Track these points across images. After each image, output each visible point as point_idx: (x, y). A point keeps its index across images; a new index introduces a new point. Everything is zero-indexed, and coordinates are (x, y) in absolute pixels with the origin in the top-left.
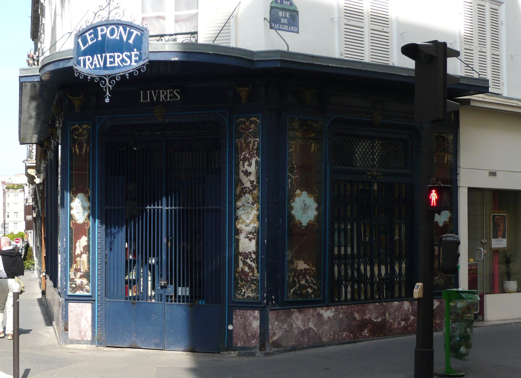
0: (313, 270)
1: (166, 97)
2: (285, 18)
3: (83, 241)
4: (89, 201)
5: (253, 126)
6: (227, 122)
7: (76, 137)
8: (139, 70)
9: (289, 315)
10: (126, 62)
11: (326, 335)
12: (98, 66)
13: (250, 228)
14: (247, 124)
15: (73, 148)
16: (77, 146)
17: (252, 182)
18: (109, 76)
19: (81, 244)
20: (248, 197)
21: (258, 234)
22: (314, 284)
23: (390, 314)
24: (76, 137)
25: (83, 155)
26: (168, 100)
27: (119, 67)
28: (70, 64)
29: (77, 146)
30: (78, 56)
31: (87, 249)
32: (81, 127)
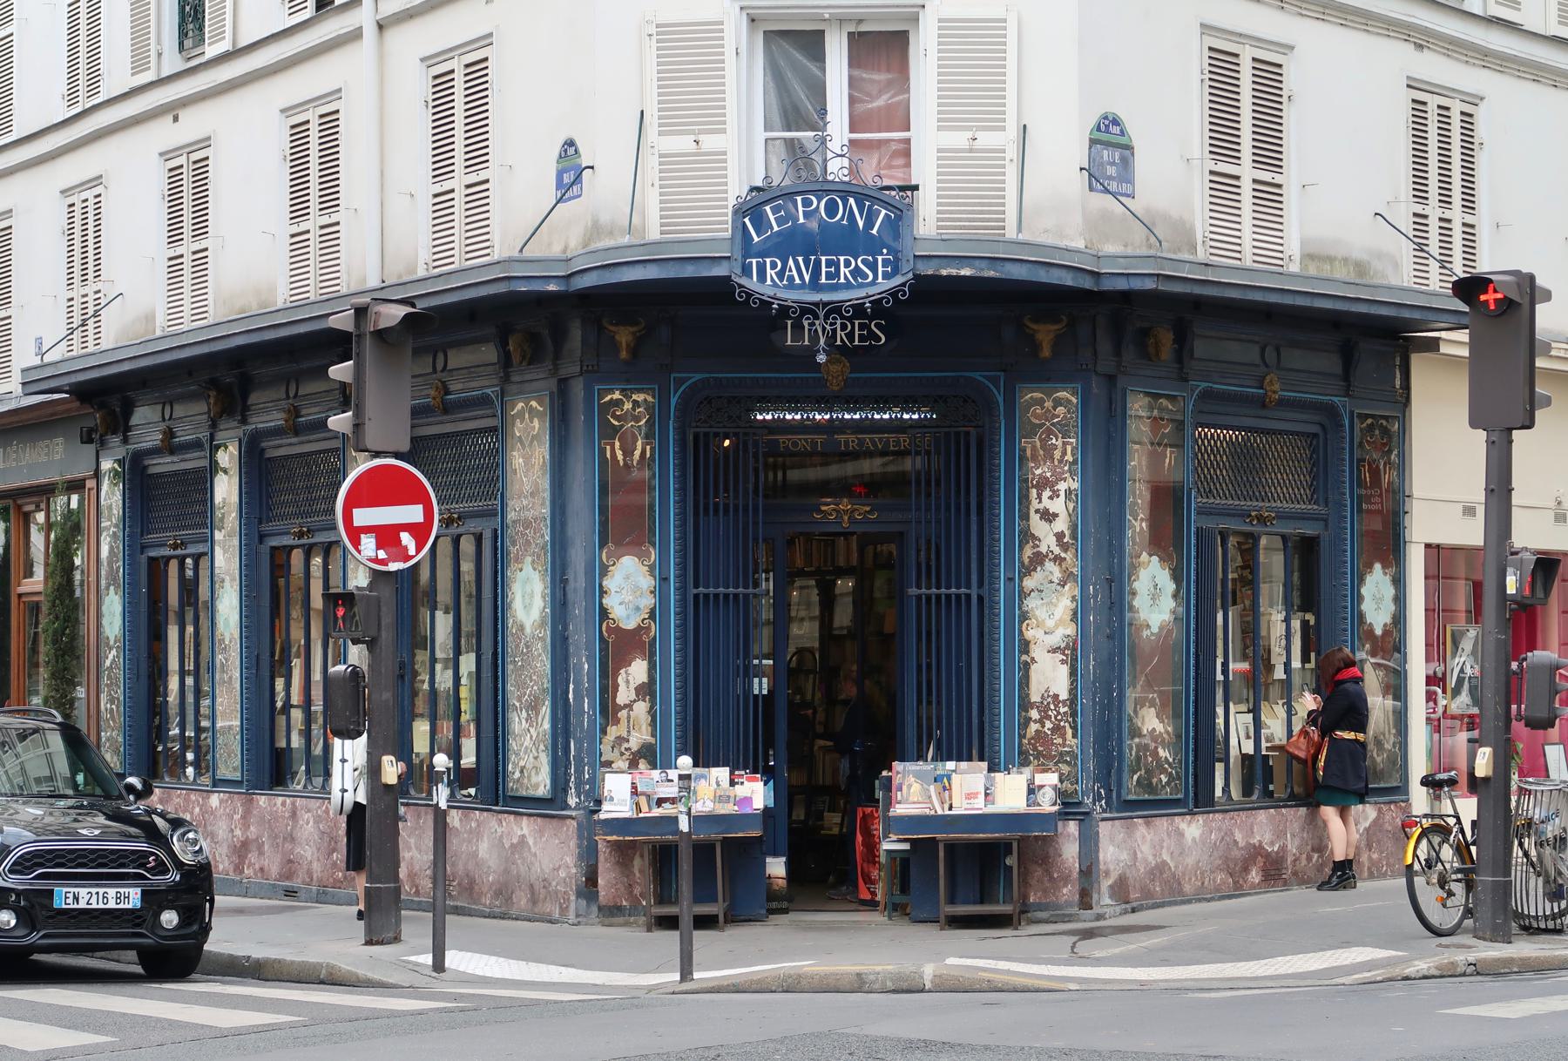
0: (1167, 732)
1: (850, 336)
2: (1113, 164)
3: (638, 671)
5: (1061, 410)
6: (1001, 400)
7: (616, 423)
8: (894, 293)
9: (1130, 831)
10: (866, 276)
11: (1190, 879)
12: (798, 281)
13: (1056, 639)
14: (1049, 404)
15: (608, 447)
16: (617, 444)
17: (1059, 536)
18: (826, 304)
19: (630, 678)
20: (1051, 569)
21: (1074, 649)
22: (1170, 764)
24: (616, 423)
25: (635, 463)
26: (856, 343)
27: (848, 286)
28: (719, 271)
29: (617, 444)
30: (745, 256)
31: (645, 691)
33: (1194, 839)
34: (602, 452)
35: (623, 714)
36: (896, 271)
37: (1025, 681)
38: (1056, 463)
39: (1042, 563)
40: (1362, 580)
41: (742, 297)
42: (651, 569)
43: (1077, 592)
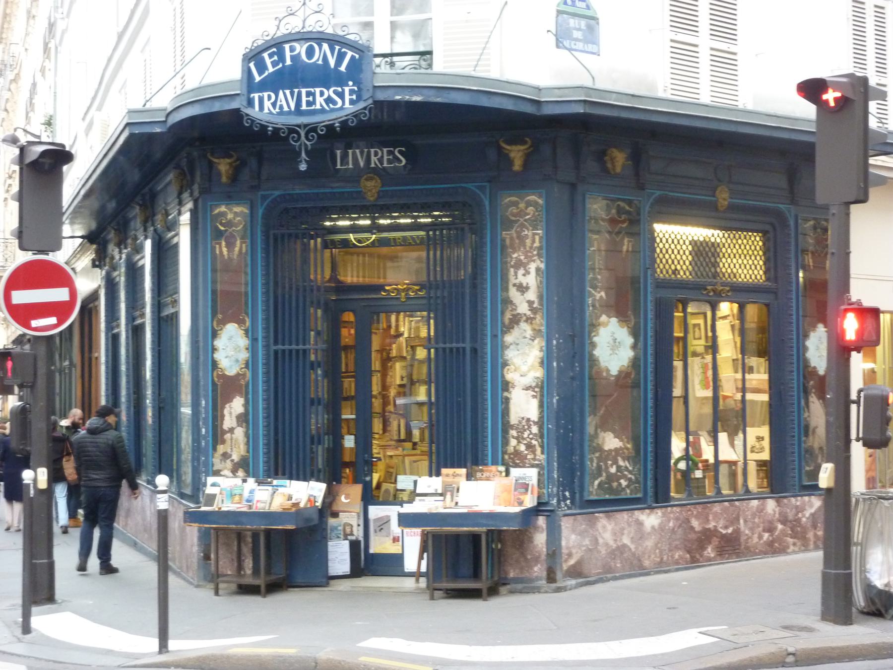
0: (627, 449)
1: (381, 160)
2: (579, 29)
3: (237, 405)
4: (247, 337)
6: (487, 203)
7: (222, 228)
8: (356, 115)
9: (592, 524)
10: (335, 103)
11: (650, 556)
12: (286, 109)
15: (217, 246)
17: (530, 303)
18: (306, 126)
20: (524, 328)
21: (542, 388)
22: (630, 472)
23: (745, 521)
24: (222, 228)
27: (323, 111)
28: (234, 105)
29: (224, 243)
30: (249, 92)
31: (243, 419)
32: (231, 210)
33: (653, 527)
34: (213, 249)
35: (228, 436)
36: (359, 98)
37: (506, 412)
38: (528, 249)
39: (517, 323)
40: (806, 336)
41: (248, 123)
42: (246, 332)
43: (544, 344)
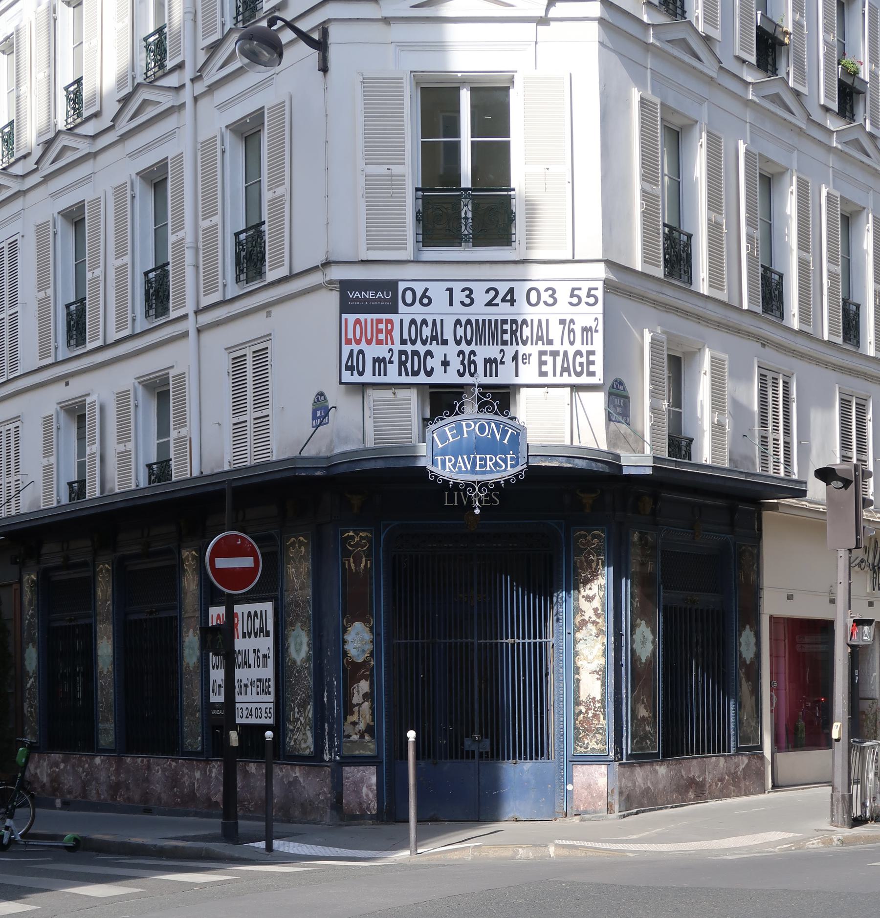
3: (364, 686)
4: (372, 633)
6: (563, 535)
7: (351, 549)
9: (632, 772)
10: (501, 467)
12: (464, 469)
14: (589, 538)
15: (347, 562)
17: (596, 610)
18: (479, 482)
19: (360, 689)
20: (591, 628)
21: (604, 672)
22: (651, 734)
23: (709, 772)
24: (351, 549)
26: (484, 504)
32: (358, 535)
33: (662, 775)
34: (343, 564)
35: (356, 709)
36: (517, 464)
37: (577, 690)
38: (593, 570)
39: (586, 626)
40: (740, 635)
41: (432, 478)
42: (371, 629)
43: (605, 641)
